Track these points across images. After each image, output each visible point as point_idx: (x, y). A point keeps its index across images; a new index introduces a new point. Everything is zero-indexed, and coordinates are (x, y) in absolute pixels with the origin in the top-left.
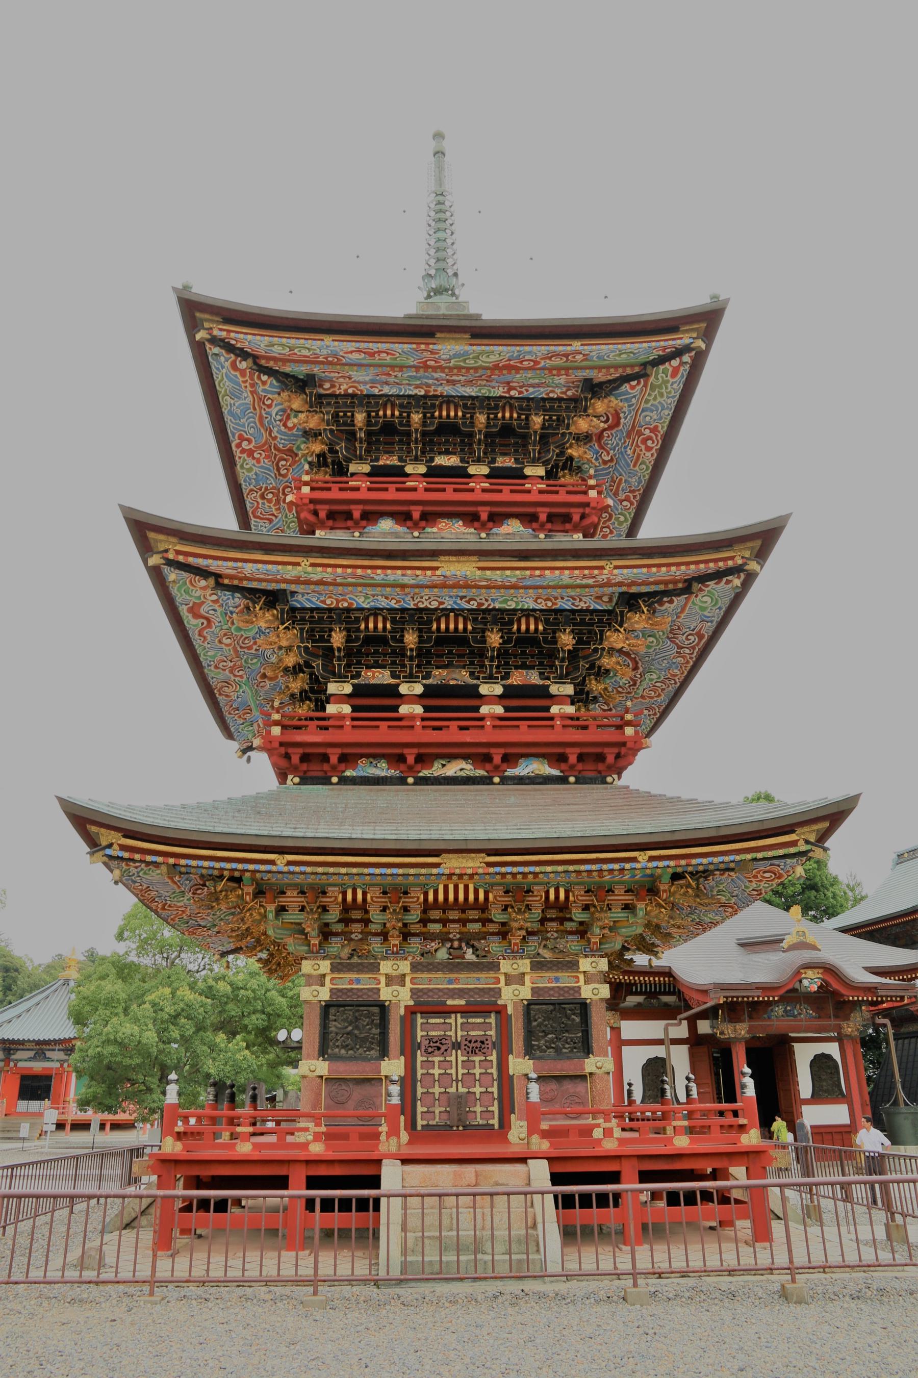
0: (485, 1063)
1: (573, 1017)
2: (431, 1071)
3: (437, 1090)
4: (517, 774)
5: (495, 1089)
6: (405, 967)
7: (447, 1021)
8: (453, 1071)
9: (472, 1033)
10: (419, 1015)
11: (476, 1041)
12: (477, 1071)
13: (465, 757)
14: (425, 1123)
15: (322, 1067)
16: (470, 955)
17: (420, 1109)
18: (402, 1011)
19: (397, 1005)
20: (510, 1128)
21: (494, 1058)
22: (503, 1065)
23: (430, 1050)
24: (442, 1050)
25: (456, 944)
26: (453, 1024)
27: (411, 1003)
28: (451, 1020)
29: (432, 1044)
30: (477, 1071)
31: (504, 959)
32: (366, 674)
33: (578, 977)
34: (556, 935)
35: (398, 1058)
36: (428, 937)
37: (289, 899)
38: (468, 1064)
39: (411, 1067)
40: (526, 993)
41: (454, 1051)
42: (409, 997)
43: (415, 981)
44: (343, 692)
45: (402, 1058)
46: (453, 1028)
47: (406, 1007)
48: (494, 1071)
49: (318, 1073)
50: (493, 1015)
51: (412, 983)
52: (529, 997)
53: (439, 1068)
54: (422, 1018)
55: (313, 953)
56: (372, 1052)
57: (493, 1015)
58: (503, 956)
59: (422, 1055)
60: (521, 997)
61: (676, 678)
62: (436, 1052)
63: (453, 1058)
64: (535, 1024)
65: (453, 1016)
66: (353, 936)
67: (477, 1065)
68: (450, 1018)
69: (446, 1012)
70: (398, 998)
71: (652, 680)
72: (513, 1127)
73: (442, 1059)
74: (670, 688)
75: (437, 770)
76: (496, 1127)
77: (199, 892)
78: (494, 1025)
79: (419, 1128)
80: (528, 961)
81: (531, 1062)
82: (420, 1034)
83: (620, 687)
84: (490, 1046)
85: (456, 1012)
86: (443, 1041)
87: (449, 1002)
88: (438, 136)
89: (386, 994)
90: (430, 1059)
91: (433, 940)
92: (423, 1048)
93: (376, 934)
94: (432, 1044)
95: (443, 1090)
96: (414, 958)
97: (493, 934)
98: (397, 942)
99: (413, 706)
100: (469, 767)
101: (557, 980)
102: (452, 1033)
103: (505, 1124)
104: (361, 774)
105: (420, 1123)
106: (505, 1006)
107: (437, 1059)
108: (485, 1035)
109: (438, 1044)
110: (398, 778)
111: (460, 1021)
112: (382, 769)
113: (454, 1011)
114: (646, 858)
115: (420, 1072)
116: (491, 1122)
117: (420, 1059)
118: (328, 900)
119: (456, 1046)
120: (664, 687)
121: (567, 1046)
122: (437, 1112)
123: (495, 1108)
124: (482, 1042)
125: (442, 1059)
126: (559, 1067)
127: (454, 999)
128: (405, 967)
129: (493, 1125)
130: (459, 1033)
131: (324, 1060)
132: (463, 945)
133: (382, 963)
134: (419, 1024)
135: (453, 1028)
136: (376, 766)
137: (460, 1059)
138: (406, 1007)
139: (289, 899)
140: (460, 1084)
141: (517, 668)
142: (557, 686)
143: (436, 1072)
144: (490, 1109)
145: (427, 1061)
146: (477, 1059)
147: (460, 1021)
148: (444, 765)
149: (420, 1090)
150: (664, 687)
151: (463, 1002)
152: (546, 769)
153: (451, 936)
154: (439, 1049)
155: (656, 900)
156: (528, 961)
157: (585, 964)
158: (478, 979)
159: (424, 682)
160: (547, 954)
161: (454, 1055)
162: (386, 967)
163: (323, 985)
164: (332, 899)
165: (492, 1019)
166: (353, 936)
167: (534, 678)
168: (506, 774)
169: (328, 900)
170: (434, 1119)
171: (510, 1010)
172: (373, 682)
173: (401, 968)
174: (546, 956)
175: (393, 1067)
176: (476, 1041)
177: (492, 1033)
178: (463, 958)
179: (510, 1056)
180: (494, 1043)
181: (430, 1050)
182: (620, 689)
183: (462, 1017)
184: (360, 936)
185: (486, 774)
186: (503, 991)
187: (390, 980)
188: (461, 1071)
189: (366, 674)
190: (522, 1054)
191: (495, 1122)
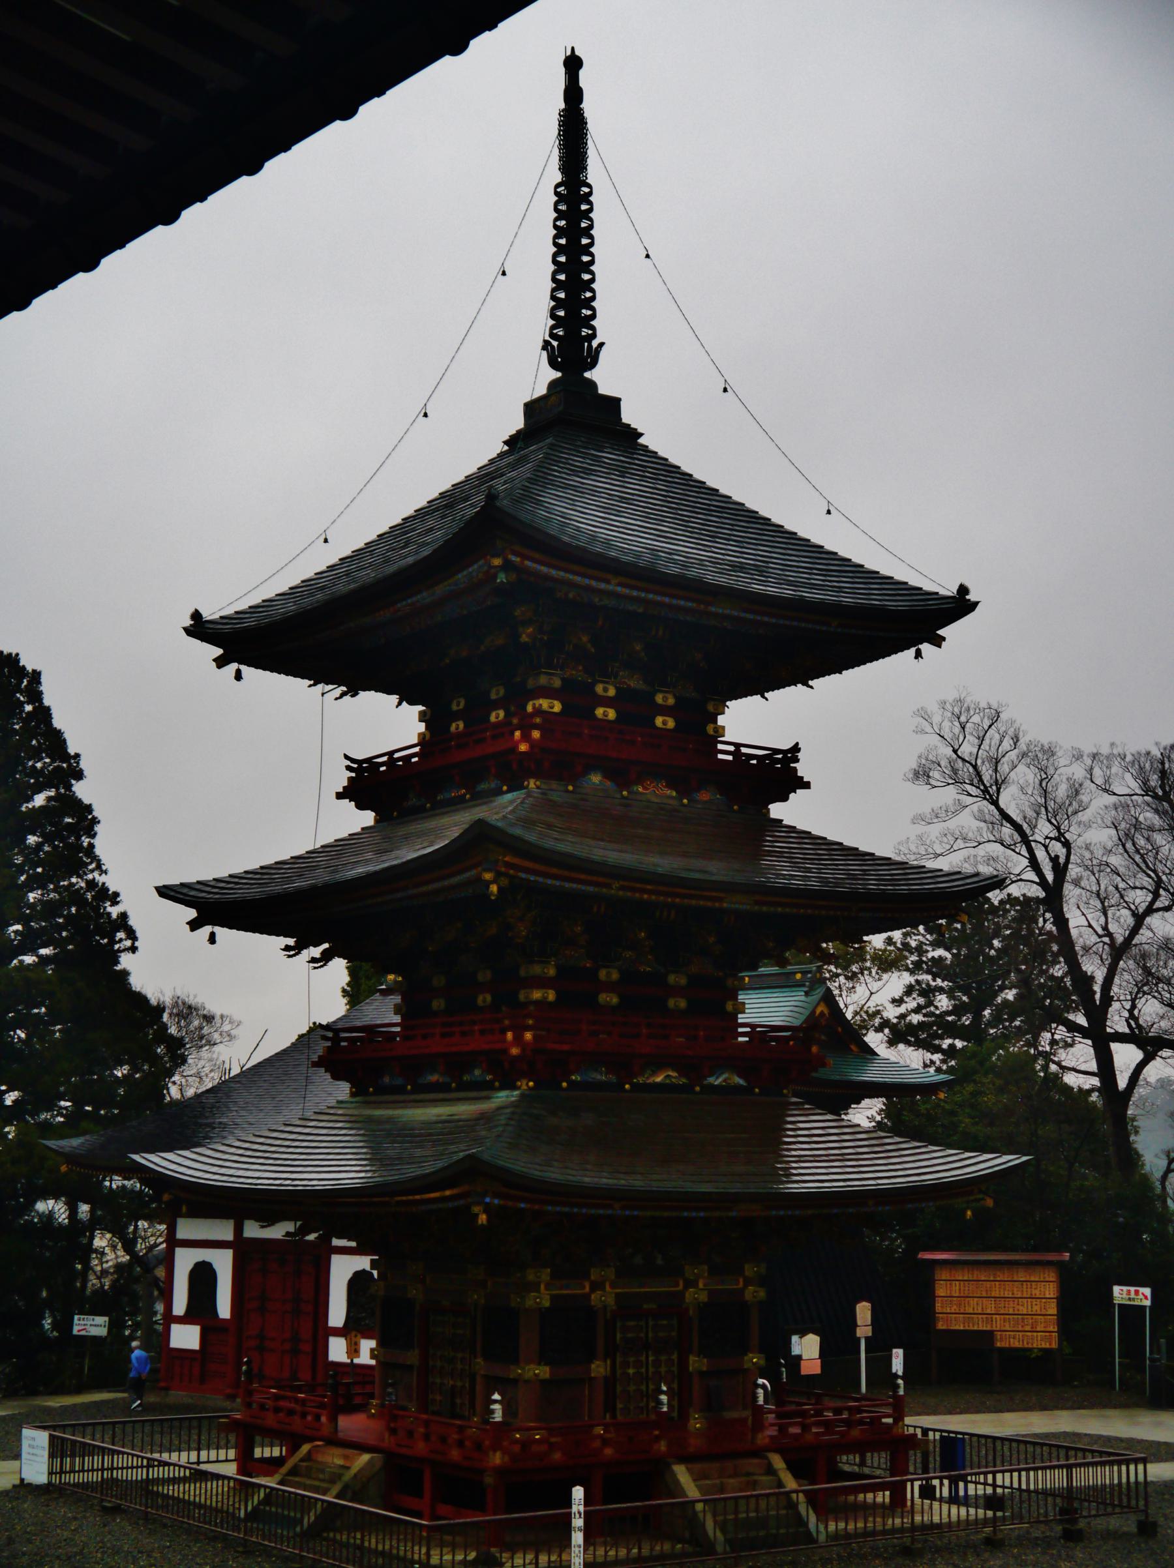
3: (632, 1388)
8: (643, 1370)
12: (663, 1369)
15: (542, 1371)
21: (675, 1357)
22: (683, 1363)
27: (614, 1308)
48: (675, 1369)
52: (706, 1300)
63: (643, 1358)
81: (705, 1360)
82: (618, 1336)
87: (645, 1306)
88: (573, 64)
100: (675, 1074)
102: (642, 1335)
107: (632, 1359)
115: (619, 1372)
117: (619, 1359)
130: (650, 1335)
131: (546, 1364)
137: (651, 1358)
143: (631, 1371)
146: (663, 1358)
147: (651, 1323)
149: (619, 1389)
151: (654, 1306)
152: (738, 1080)
171: (691, 1312)
175: (599, 1369)
177: (674, 1334)
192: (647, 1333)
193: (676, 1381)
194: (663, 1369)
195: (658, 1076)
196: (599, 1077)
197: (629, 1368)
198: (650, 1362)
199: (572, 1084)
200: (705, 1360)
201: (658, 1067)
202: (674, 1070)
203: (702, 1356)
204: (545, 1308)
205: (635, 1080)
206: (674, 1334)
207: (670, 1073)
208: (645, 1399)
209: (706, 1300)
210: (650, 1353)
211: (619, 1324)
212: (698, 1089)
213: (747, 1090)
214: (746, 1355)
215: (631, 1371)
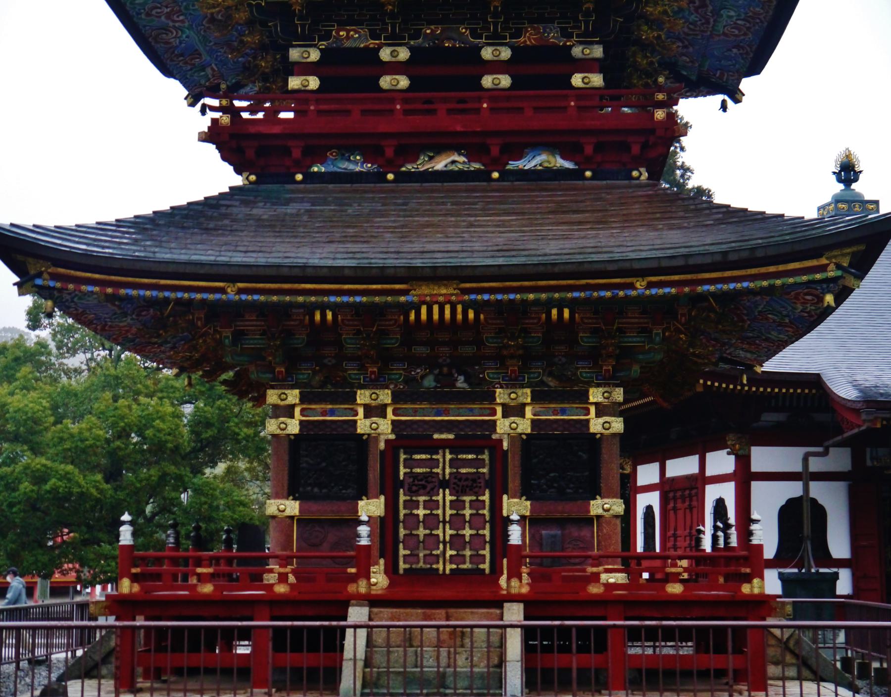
0: (477, 505)
1: (580, 453)
2: (415, 512)
4: (521, 167)
5: (487, 532)
6: (385, 396)
7: (434, 457)
8: (440, 512)
9: (463, 471)
10: (402, 450)
11: (467, 479)
12: (467, 512)
13: (457, 149)
14: (407, 566)
15: (292, 507)
16: (461, 383)
17: (402, 552)
18: (382, 445)
19: (376, 439)
21: (486, 498)
22: (496, 506)
23: (414, 488)
24: (428, 489)
25: (445, 370)
26: (441, 460)
27: (392, 437)
28: (439, 457)
29: (416, 482)
31: (501, 387)
32: (338, 33)
33: (588, 410)
34: (564, 360)
35: (377, 497)
36: (416, 361)
37: (247, 323)
38: (457, 505)
39: (392, 506)
40: (524, 426)
41: (441, 491)
42: (390, 431)
43: (399, 412)
44: (309, 60)
45: (382, 498)
46: (441, 465)
47: (387, 442)
48: (486, 512)
49: (288, 512)
50: (486, 452)
51: (394, 414)
52: (529, 431)
53: (425, 508)
54: (405, 454)
55: (278, 380)
56: (349, 491)
57: (486, 452)
58: (499, 383)
59: (405, 495)
60: (519, 430)
61: (761, 17)
62: (422, 491)
64: (535, 461)
66: (326, 361)
67: (467, 505)
68: (438, 453)
69: (435, 447)
70: (377, 431)
71: (731, 17)
73: (427, 498)
74: (757, 27)
75: (423, 165)
76: (487, 571)
77: (144, 313)
78: (487, 462)
79: (401, 572)
81: (528, 503)
82: (402, 471)
83: (691, 23)
84: (482, 484)
85: (444, 448)
86: (430, 479)
87: (436, 436)
89: (363, 426)
90: (414, 498)
91: (419, 366)
92: (406, 487)
94: (416, 482)
95: (428, 532)
96: (396, 386)
98: (375, 369)
99: (397, 77)
100: (462, 159)
101: (563, 412)
102: (439, 470)
103: (496, 570)
104: (332, 169)
105: (402, 566)
106: (500, 441)
108: (478, 472)
109: (423, 482)
110: (374, 173)
111: (448, 457)
112: (356, 165)
113: (444, 445)
114: (644, 283)
115: (402, 512)
117: (402, 498)
118: (292, 323)
119: (444, 484)
120: (748, 25)
121: (572, 486)
122: (421, 555)
123: (486, 552)
124: (474, 481)
125: (427, 498)
126: (560, 508)
127: (441, 433)
128: (385, 396)
130: (448, 471)
131: (295, 499)
132: (454, 371)
134: (402, 460)
135: (441, 465)
136: (349, 160)
138: (387, 442)
139: (247, 323)
140: (448, 526)
141: (532, 21)
142: (581, 48)
143: (421, 512)
144: (481, 552)
145: (411, 500)
146: (467, 499)
148: (431, 158)
149: (402, 532)
150: (748, 25)
152: (561, 163)
153: (440, 360)
154: (424, 487)
155: (674, 325)
156: (528, 391)
157: (596, 395)
158: (471, 410)
159: (412, 43)
160: (552, 383)
161: (441, 495)
162: (363, 397)
163: (292, 416)
164: (297, 323)
165: (486, 456)
166: (326, 361)
167: (553, 36)
168: (508, 167)
169: (292, 323)
171: (505, 445)
172: (348, 44)
173: (381, 397)
174: (551, 384)
176: (467, 479)
178: (454, 386)
179: (505, 497)
180: (486, 481)
181: (414, 488)
182: (691, 27)
183: (451, 453)
184: (334, 361)
185: (483, 168)
186: (498, 423)
187: (370, 411)
188: (449, 512)
189: (338, 33)
190: (518, 494)
191: (486, 566)
192: (444, 469)
193: (488, 526)
194: (467, 512)
195: (438, 163)
196: (351, 167)
197: (418, 508)
198: (448, 504)
199: (310, 177)
200: (528, 503)
201: (439, 149)
202: (460, 154)
203: (524, 498)
204: (294, 435)
205: (404, 169)
206: (485, 470)
207: (456, 157)
208: (441, 546)
209: (529, 431)
210: (447, 491)
211: (403, 457)
212: (496, 175)
213: (577, 174)
214: (595, 499)
215: (421, 512)
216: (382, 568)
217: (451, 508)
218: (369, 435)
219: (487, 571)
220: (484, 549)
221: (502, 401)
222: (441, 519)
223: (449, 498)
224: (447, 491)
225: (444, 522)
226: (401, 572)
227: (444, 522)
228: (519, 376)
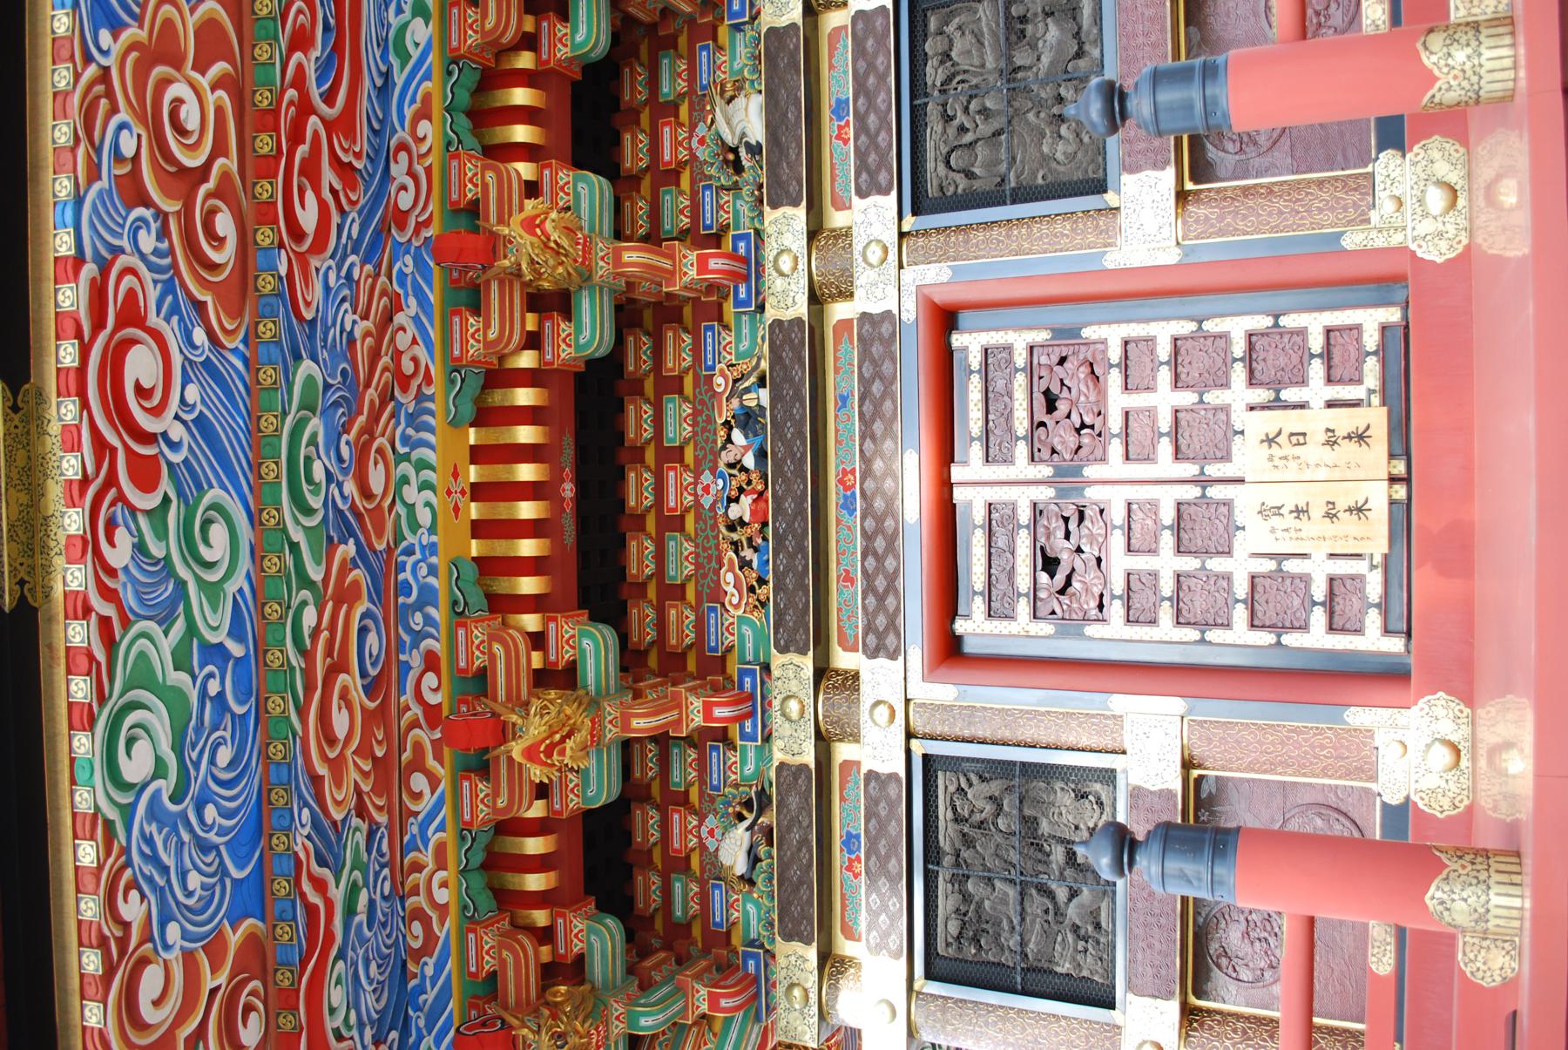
12: (1164, 399)
14: (1373, 620)
20: (1403, 250)
30: (1164, 399)
34: (701, 130)
48: (1163, 333)
60: (891, 237)
65: (959, 495)
72: (1396, 239)
73: (1117, 540)
79: (1395, 645)
80: (770, 215)
93: (703, 766)
97: (697, 350)
105: (1374, 640)
116: (1371, 340)
129: (1384, 328)
133: (778, 756)
143: (1167, 563)
153: (707, 501)
156: (770, 215)
170: (1358, 579)
173: (794, 686)
177: (1019, 341)
188: (1165, 463)
191: (1371, 320)
197: (1155, 575)
216: (1385, 713)
217: (1149, 458)
218: (910, 735)
219: (1393, 315)
220: (1302, 332)
221: (803, 299)
222: (1192, 492)
223: (1115, 466)
224: (1091, 472)
225: (1203, 482)
226: (1395, 645)
227: (1203, 482)
228: (735, 248)
